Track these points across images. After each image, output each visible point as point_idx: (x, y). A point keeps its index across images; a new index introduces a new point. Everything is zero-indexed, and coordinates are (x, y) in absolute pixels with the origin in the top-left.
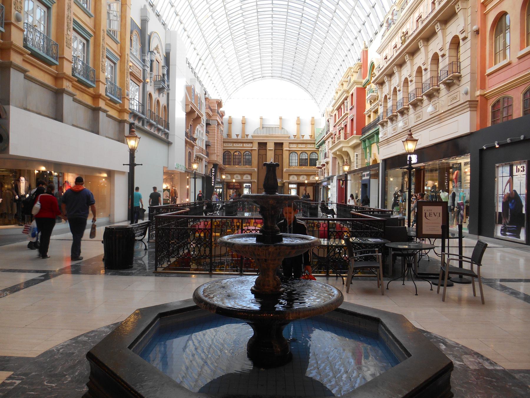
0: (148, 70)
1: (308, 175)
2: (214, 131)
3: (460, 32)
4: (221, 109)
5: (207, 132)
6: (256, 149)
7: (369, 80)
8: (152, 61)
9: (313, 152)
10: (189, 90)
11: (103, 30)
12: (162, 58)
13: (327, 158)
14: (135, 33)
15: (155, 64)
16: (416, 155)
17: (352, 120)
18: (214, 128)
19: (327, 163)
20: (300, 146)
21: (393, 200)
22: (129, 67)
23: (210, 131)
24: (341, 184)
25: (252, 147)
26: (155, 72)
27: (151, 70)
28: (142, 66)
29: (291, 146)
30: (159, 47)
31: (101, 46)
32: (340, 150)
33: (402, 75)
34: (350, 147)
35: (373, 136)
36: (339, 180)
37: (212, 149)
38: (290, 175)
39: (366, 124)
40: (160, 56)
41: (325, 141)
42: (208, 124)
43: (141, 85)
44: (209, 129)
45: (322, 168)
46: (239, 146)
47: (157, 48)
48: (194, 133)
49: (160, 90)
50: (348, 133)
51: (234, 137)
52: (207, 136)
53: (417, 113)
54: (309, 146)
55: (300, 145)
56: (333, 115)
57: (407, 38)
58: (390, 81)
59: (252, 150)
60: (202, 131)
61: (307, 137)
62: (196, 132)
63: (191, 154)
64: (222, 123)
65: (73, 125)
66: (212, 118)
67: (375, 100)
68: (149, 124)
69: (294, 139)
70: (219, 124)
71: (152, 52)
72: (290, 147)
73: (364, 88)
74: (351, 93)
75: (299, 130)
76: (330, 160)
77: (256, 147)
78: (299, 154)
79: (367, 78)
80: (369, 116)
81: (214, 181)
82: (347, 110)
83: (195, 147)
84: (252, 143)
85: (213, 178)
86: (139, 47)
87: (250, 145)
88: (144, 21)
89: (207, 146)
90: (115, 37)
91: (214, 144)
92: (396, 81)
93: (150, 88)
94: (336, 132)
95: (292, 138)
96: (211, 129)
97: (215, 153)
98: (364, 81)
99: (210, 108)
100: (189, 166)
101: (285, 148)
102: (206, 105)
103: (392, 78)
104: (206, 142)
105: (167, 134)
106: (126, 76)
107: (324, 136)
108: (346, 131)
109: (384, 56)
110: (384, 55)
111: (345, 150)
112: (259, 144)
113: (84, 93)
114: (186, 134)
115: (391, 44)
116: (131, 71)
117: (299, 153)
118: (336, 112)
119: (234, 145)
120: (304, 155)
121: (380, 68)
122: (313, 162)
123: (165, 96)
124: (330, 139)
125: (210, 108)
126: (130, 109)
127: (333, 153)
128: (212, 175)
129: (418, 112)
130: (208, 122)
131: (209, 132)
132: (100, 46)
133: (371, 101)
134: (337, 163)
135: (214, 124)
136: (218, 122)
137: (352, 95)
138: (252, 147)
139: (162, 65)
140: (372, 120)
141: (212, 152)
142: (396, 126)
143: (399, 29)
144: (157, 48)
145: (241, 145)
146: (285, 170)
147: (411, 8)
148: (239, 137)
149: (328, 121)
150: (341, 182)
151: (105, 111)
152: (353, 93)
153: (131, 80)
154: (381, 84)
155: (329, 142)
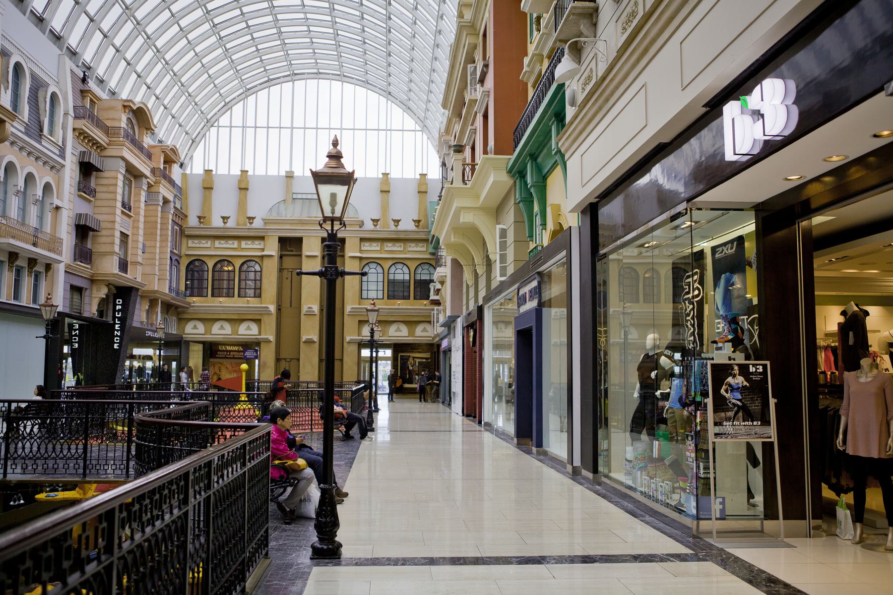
1: (411, 323)
2: (111, 189)
6: (273, 253)
9: (423, 263)
18: (113, 181)
20: (389, 246)
21: (636, 395)
25: (263, 250)
29: (366, 246)
46: (228, 246)
54: (413, 247)
55: (390, 244)
59: (262, 257)
61: (407, 225)
69: (372, 227)
72: (363, 248)
75: (385, 207)
77: (272, 248)
78: (386, 267)
81: (121, 337)
84: (262, 238)
85: (117, 327)
87: (257, 244)
91: (109, 225)
95: (369, 225)
96: (104, 181)
97: (113, 253)
111: (466, 220)
112: (283, 241)
117: (386, 265)
119: (217, 243)
120: (399, 271)
122: (423, 289)
128: (114, 317)
130: (86, 160)
138: (263, 250)
141: (103, 248)
145: (235, 244)
146: (348, 309)
148: (231, 223)
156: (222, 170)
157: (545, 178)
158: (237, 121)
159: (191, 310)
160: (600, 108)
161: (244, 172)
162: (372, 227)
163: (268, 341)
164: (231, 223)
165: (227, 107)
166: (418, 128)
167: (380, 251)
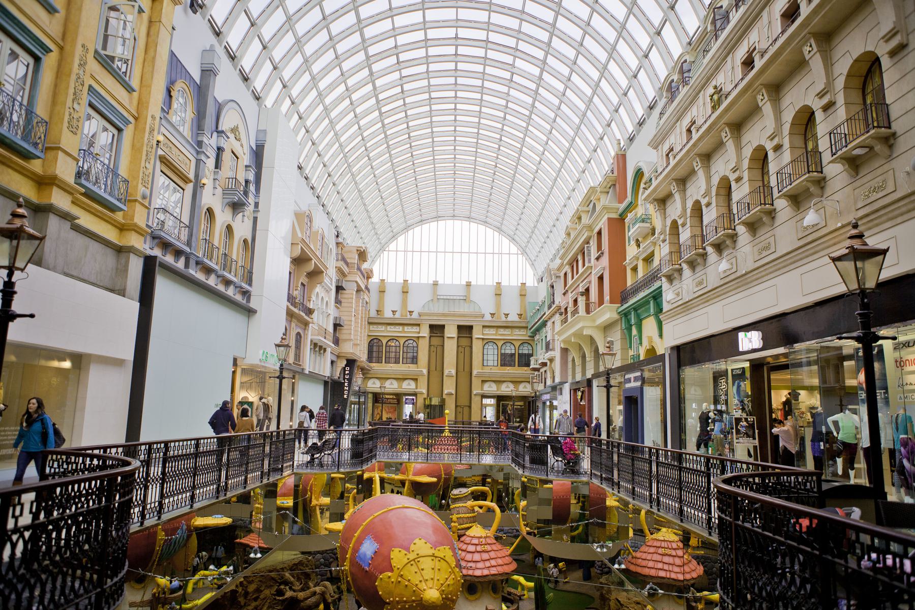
0: (211, 163)
1: (516, 383)
2: (350, 300)
3: (817, 95)
4: (365, 266)
5: (338, 301)
7: (631, 203)
8: (220, 150)
9: (524, 343)
10: (303, 219)
11: (83, 46)
12: (247, 150)
13: (551, 350)
14: (179, 85)
15: (227, 156)
16: (760, 333)
17: (601, 278)
18: (351, 296)
19: (551, 360)
20: (502, 331)
21: (698, 429)
22: (155, 143)
23: (343, 300)
24: (579, 397)
25: (419, 333)
26: (227, 171)
27: (218, 165)
28: (195, 155)
29: (487, 331)
30: (242, 129)
31: (73, 77)
32: (578, 334)
33: (712, 174)
34: (597, 327)
35: (648, 302)
36: (575, 390)
37: (344, 331)
38: (483, 382)
39: (629, 283)
40: (242, 145)
41: (547, 321)
42: (339, 288)
43: (189, 188)
44: (344, 296)
45: (541, 370)
47: (235, 130)
48: (309, 301)
49: (236, 207)
50: (593, 301)
51: (388, 314)
52: (338, 308)
53: (757, 241)
54: (517, 332)
55: (502, 330)
56: (562, 275)
57: (723, 97)
58: (684, 190)
59: (418, 337)
60: (326, 299)
61: (513, 317)
62: (314, 298)
63: (301, 337)
64: (367, 288)
65: (67, 275)
66: (348, 278)
67: (645, 237)
68: (199, 266)
69: (490, 319)
70: (359, 290)
71: (220, 133)
73: (622, 218)
74: (596, 230)
75: (498, 305)
76: (557, 354)
77: (425, 332)
78: (500, 346)
79: (629, 199)
80: (635, 269)
81: (349, 391)
82: (590, 261)
83: (310, 325)
84: (419, 325)
85: (346, 384)
86: (189, 115)
87: (415, 329)
88: (208, 72)
89: (337, 326)
90: (127, 79)
91: (349, 323)
92: (698, 189)
93: (211, 198)
94: (568, 303)
95: (488, 317)
96: (346, 296)
97: (351, 340)
98: (622, 206)
99: (344, 259)
100: (295, 359)
101: (477, 334)
102: (337, 254)
103: (688, 185)
104: (336, 318)
105: (246, 294)
106: (144, 157)
107: (545, 314)
108: (588, 299)
109: (664, 151)
110: (666, 147)
111: (588, 333)
112: (432, 327)
113: (9, 167)
114: (291, 299)
115: (681, 125)
116: (163, 153)
117: (500, 344)
118: (567, 269)
120: (508, 348)
121: (659, 172)
122: (525, 360)
123: (249, 223)
124: (557, 315)
125: (344, 259)
126: (147, 226)
127: (564, 341)
129: (762, 238)
130: (340, 285)
131: (341, 302)
132: (69, 76)
133: (637, 240)
134: (570, 359)
135: (350, 289)
136: (358, 286)
137: (599, 233)
138: (419, 333)
139: (245, 164)
140: (641, 273)
142: (704, 277)
143: (700, 91)
144: (235, 130)
145: (401, 329)
146: (475, 372)
147: (727, 42)
148: (397, 315)
149: (553, 287)
150: (579, 394)
151: (65, 216)
152: (600, 230)
153: (161, 171)
154: (663, 202)
155: (553, 323)
156: (391, 280)
157: (641, 320)
158: (401, 247)
159: (372, 372)
160: (684, 311)
161: (406, 281)
162: (490, 319)
163: (422, 393)
164: (397, 315)
165: (394, 237)
166: (519, 252)
167: (495, 334)
